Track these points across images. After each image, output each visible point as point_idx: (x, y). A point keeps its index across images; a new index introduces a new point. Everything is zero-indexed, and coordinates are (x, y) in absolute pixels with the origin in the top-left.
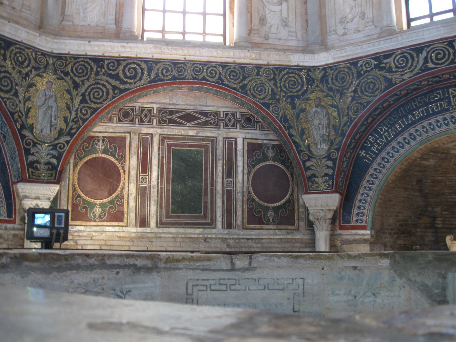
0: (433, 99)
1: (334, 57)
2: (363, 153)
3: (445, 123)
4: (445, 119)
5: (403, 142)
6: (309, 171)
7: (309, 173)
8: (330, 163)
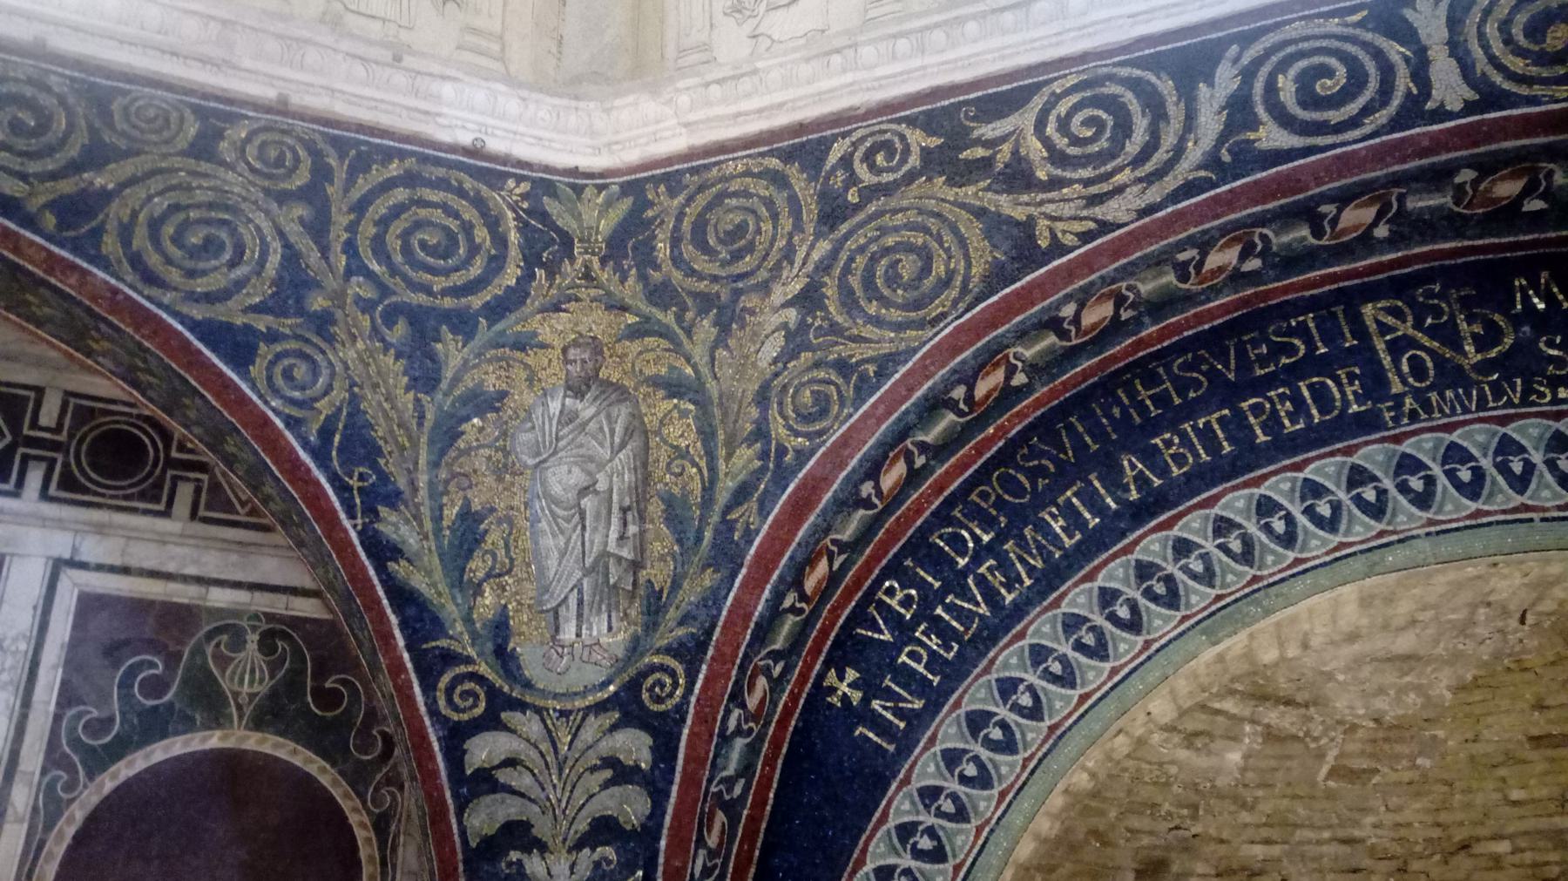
0: (1263, 361)
1: (692, 117)
2: (845, 686)
3: (1359, 501)
4: (1358, 477)
5: (1099, 620)
6: (488, 799)
7: (485, 817)
8: (635, 746)
